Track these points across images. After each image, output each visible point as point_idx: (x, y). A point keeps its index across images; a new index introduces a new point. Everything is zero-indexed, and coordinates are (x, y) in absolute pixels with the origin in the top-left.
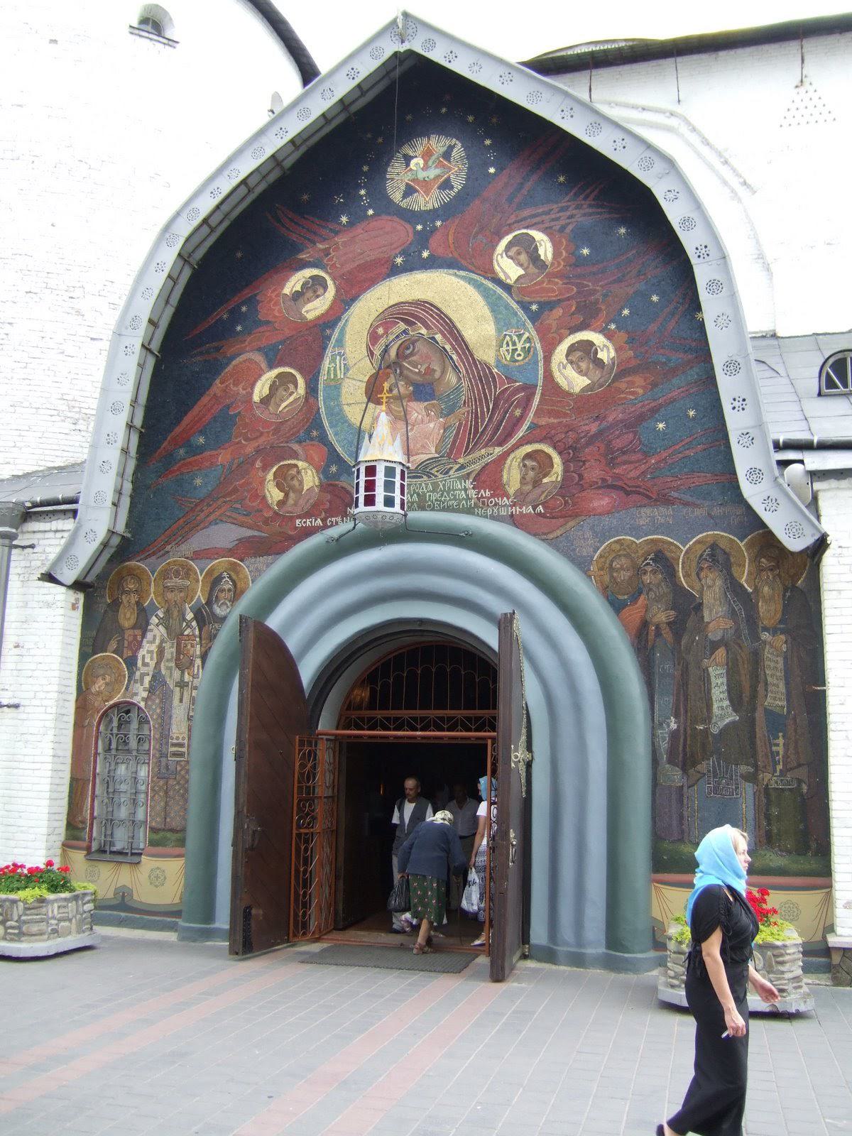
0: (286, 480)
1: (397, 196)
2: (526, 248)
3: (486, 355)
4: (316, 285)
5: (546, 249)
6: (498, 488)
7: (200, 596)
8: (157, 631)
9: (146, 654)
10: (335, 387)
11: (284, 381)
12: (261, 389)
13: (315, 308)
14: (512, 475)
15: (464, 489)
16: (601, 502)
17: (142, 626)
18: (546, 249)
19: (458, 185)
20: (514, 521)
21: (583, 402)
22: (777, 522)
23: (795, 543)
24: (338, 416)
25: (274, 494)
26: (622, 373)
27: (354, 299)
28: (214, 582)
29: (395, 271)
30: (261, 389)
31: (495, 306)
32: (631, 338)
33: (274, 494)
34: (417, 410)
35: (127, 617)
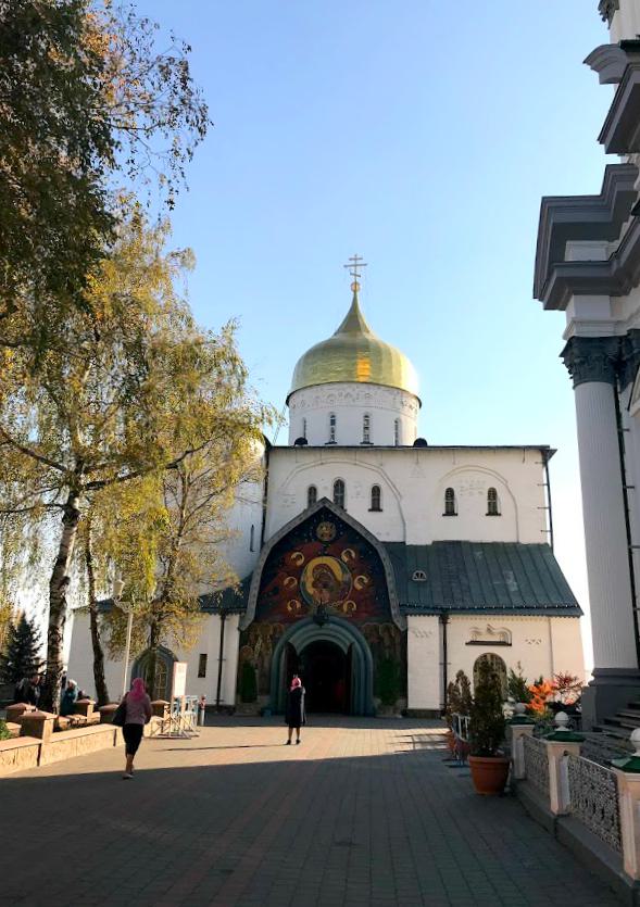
0: (293, 605)
1: (319, 536)
2: (349, 554)
3: (340, 578)
4: (299, 557)
5: (353, 555)
6: (343, 611)
7: (271, 632)
8: (260, 640)
9: (258, 646)
10: (304, 584)
11: (292, 580)
12: (286, 582)
13: (300, 563)
14: (345, 608)
15: (335, 611)
16: (365, 615)
17: (256, 639)
18: (353, 555)
19: (334, 536)
20: (346, 619)
21: (361, 592)
22: (399, 625)
23: (402, 630)
24: (305, 591)
25: (290, 608)
26: (369, 586)
27: (308, 562)
28: (275, 630)
29: (319, 556)
30: (286, 582)
31: (342, 567)
32: (369, 576)
33: (290, 608)
34: (324, 590)
35: (252, 638)
